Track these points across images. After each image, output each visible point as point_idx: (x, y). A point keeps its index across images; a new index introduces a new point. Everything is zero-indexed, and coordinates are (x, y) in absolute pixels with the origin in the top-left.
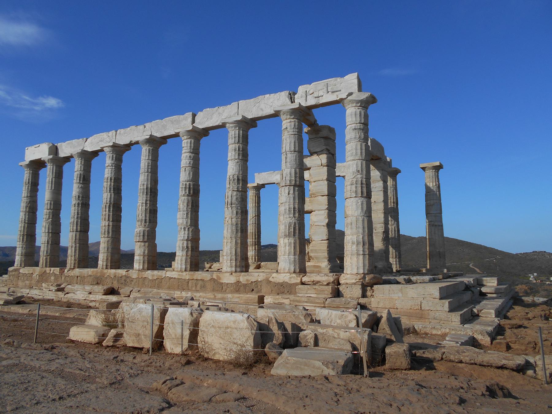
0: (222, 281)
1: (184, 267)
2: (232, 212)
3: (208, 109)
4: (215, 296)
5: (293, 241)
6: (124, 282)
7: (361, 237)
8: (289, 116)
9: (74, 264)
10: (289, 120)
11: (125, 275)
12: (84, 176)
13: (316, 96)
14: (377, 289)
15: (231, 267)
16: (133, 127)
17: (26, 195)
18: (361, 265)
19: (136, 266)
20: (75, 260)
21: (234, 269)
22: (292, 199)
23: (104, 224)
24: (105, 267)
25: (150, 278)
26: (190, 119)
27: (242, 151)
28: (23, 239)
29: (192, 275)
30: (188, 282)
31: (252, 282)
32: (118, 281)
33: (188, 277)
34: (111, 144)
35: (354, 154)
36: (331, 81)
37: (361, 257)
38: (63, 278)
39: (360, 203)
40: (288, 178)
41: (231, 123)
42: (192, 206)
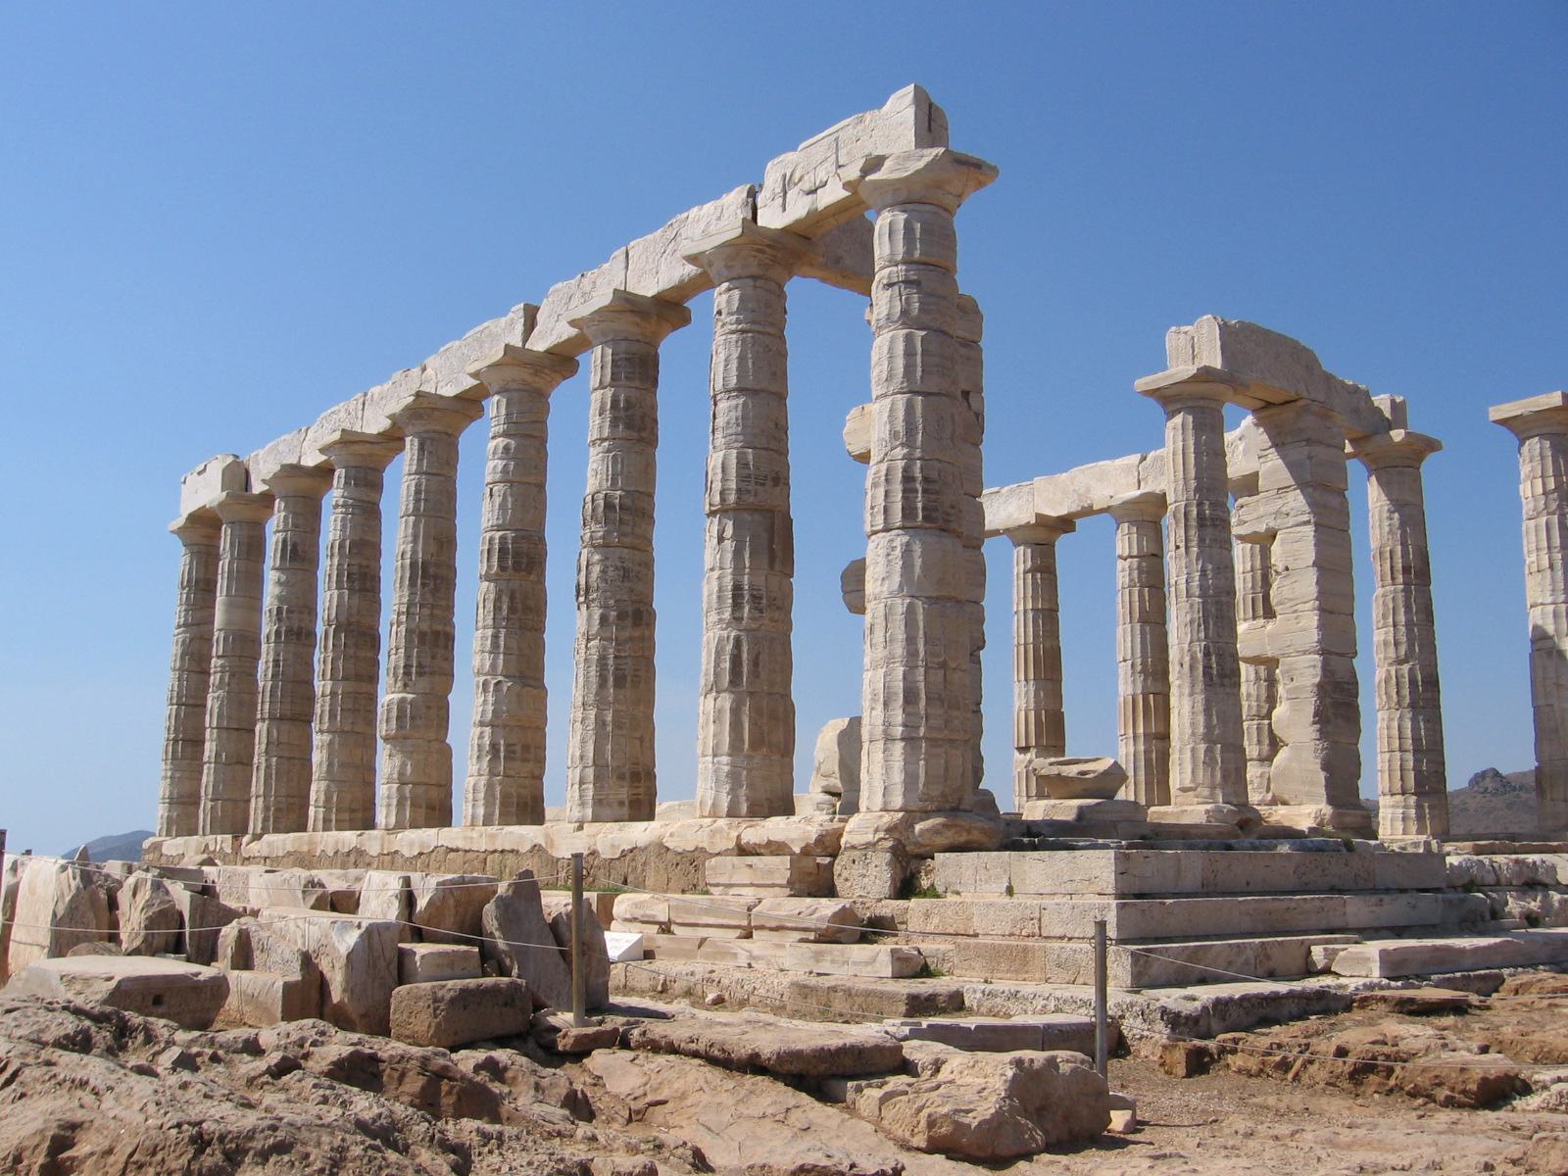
1: (481, 811)
2: (590, 617)
3: (559, 285)
5: (727, 705)
7: (900, 671)
12: (294, 546)
13: (807, 185)
14: (943, 865)
15: (583, 804)
18: (898, 777)
19: (381, 817)
21: (589, 812)
22: (729, 556)
24: (320, 824)
26: (520, 328)
27: (626, 409)
31: (623, 854)
33: (483, 845)
34: (337, 436)
35: (884, 376)
37: (898, 748)
39: (898, 552)
40: (717, 486)
42: (512, 609)
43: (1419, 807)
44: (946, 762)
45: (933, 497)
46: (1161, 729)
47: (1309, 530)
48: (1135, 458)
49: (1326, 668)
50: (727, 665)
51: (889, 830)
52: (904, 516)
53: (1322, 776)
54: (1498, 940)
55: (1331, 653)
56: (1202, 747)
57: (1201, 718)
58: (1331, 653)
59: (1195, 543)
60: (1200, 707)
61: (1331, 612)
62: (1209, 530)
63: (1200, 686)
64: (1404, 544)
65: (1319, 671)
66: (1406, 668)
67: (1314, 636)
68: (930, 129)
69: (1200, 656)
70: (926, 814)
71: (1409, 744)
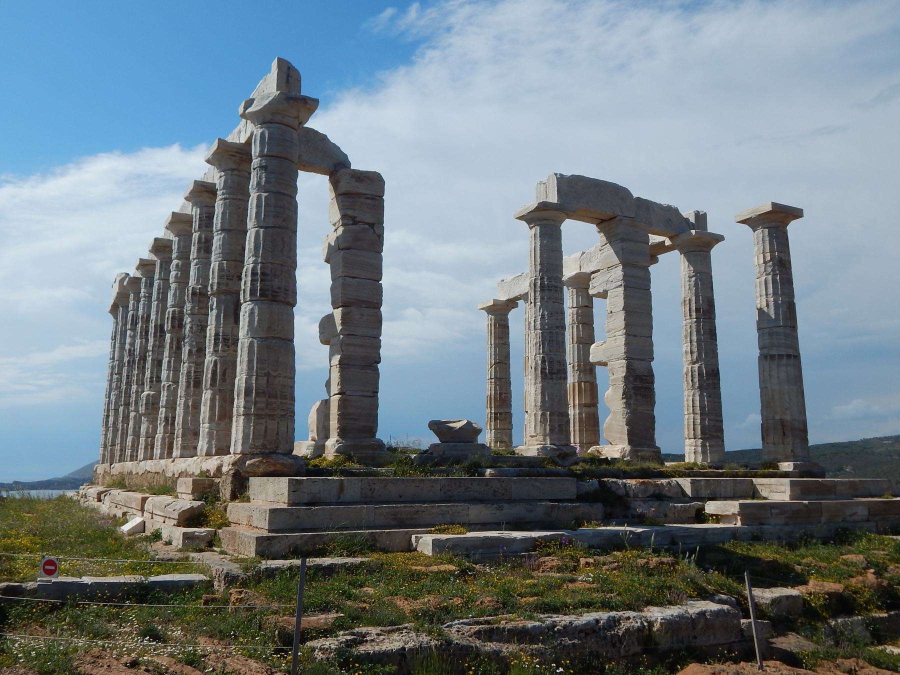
27: (205, 243)
43: (703, 446)
44: (266, 427)
45: (267, 283)
46: (588, 401)
47: (622, 288)
49: (629, 368)
50: (210, 376)
51: (233, 464)
52: (251, 295)
53: (626, 428)
54: (549, 533)
55: (634, 359)
56: (540, 413)
57: (539, 397)
58: (634, 359)
59: (538, 300)
60: (539, 391)
61: (635, 336)
62: (547, 293)
63: (539, 379)
64: (697, 295)
65: (625, 369)
66: (696, 366)
67: (622, 349)
68: (288, 81)
69: (539, 362)
70: (253, 455)
71: (698, 411)
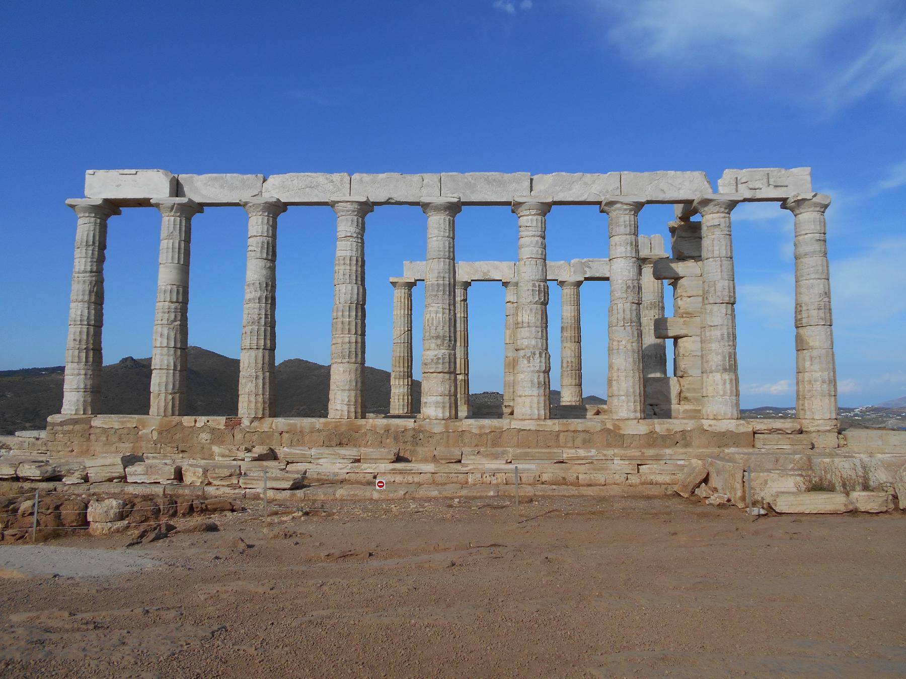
0: (622, 432)
2: (633, 333)
3: (564, 173)
4: (643, 453)
6: (410, 439)
8: (722, 209)
9: (264, 409)
10: (723, 215)
11: (414, 429)
13: (751, 186)
16: (396, 175)
17: (83, 267)
20: (264, 402)
23: (347, 340)
25: (474, 431)
28: (87, 357)
29: (564, 424)
30: (558, 436)
31: (676, 432)
32: (396, 439)
33: (557, 428)
36: (774, 171)
38: (239, 436)
41: (627, 204)
48: (512, 263)
